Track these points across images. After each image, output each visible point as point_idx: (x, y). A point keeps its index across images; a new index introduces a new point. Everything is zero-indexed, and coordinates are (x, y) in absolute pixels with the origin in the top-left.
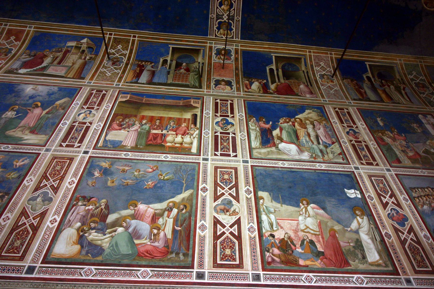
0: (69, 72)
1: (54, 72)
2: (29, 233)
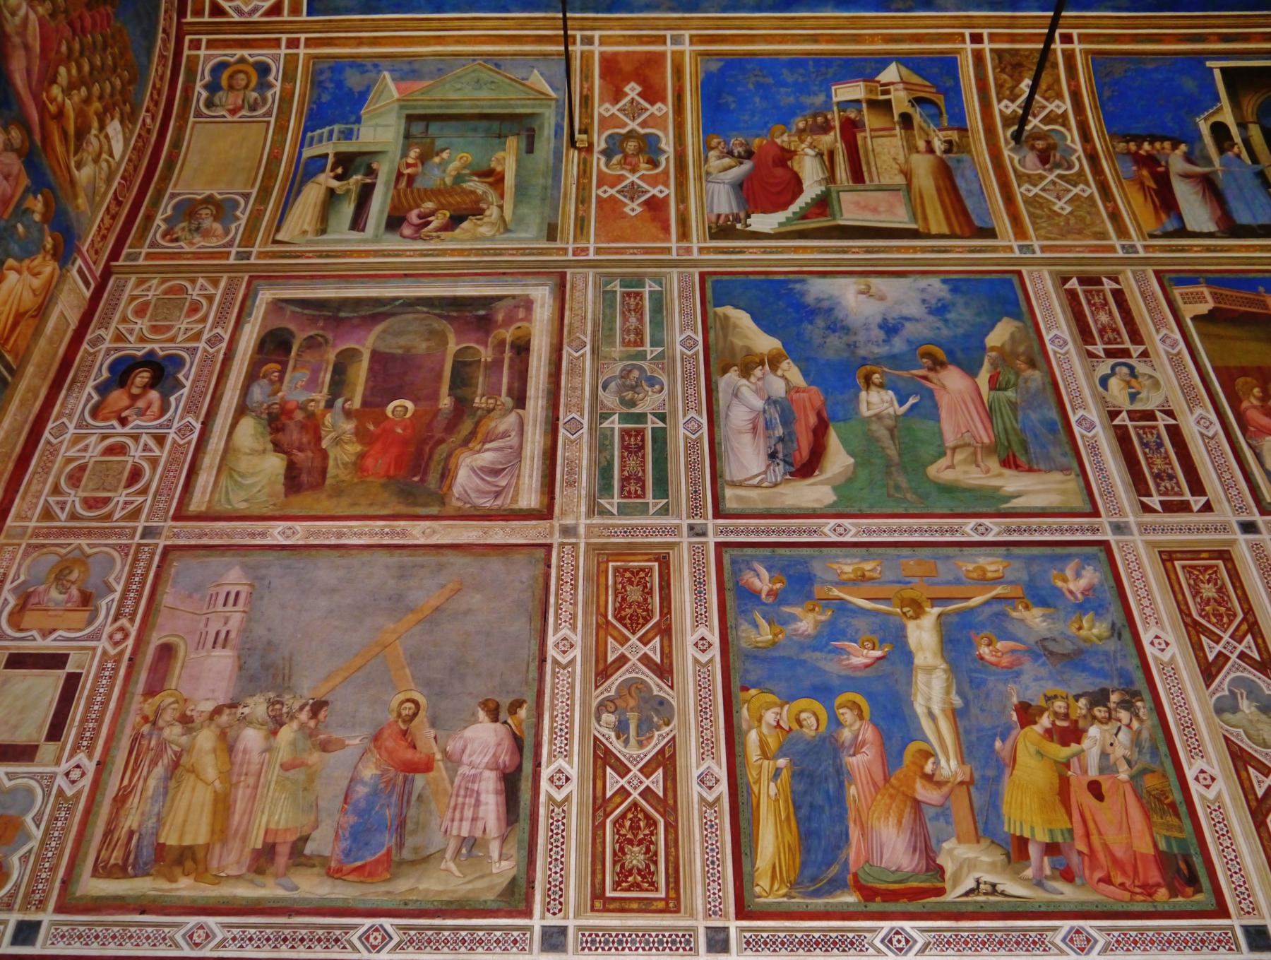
0: (919, 211)
1: (869, 216)
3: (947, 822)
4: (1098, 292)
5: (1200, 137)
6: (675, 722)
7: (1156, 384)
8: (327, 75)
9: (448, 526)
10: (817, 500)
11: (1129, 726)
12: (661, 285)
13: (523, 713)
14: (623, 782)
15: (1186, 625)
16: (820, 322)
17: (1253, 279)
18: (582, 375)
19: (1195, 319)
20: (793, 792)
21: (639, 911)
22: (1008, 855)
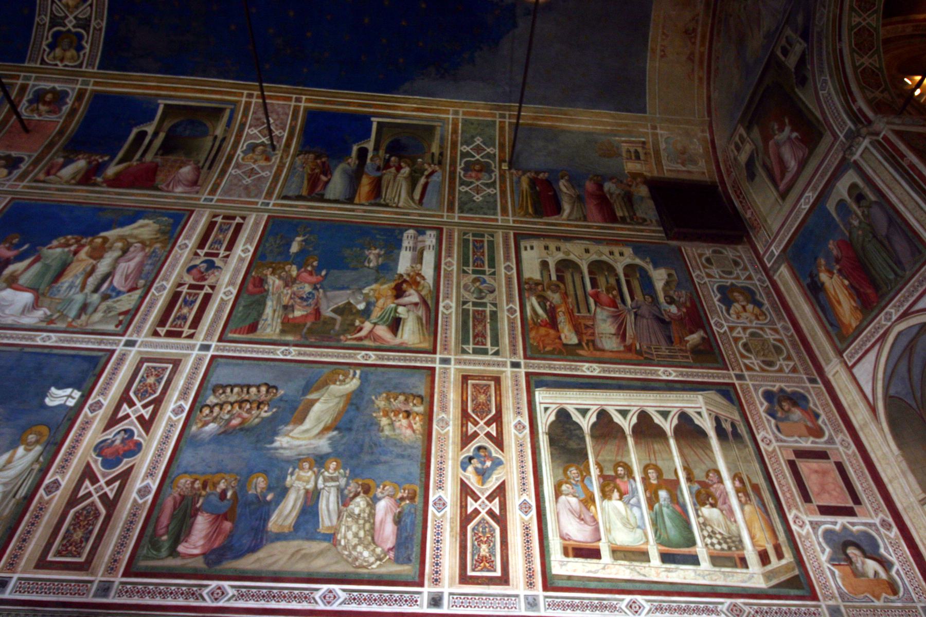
2: (494, 530)
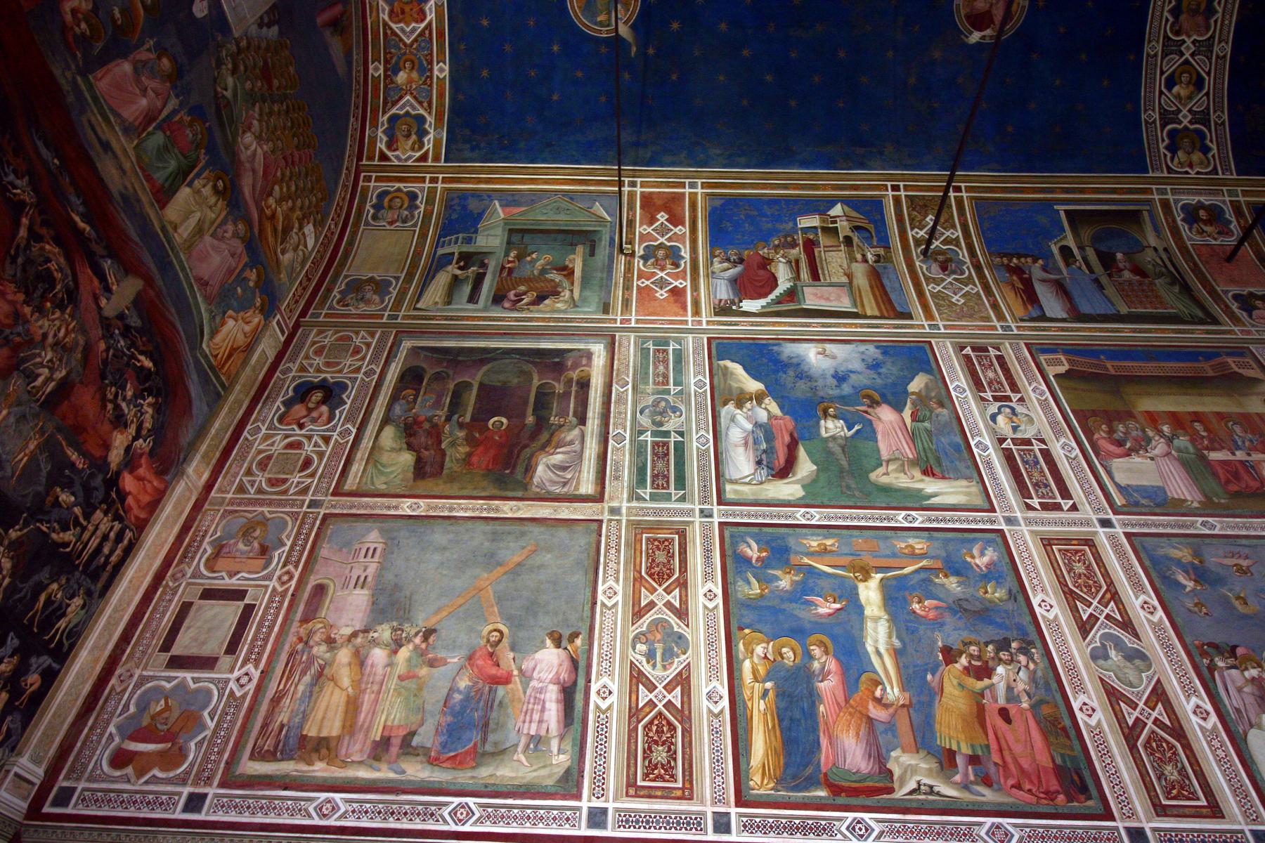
0: (858, 300)
1: (823, 302)
3: (894, 736)
4: (986, 357)
5: (1052, 254)
6: (690, 652)
7: (1031, 421)
8: (456, 201)
9: (529, 505)
10: (791, 495)
11: (1027, 667)
12: (681, 345)
13: (578, 642)
14: (651, 696)
15: (1064, 592)
16: (791, 373)
17: (1096, 351)
18: (626, 404)
19: (1056, 376)
20: (777, 708)
21: (662, 797)
22: (940, 763)
